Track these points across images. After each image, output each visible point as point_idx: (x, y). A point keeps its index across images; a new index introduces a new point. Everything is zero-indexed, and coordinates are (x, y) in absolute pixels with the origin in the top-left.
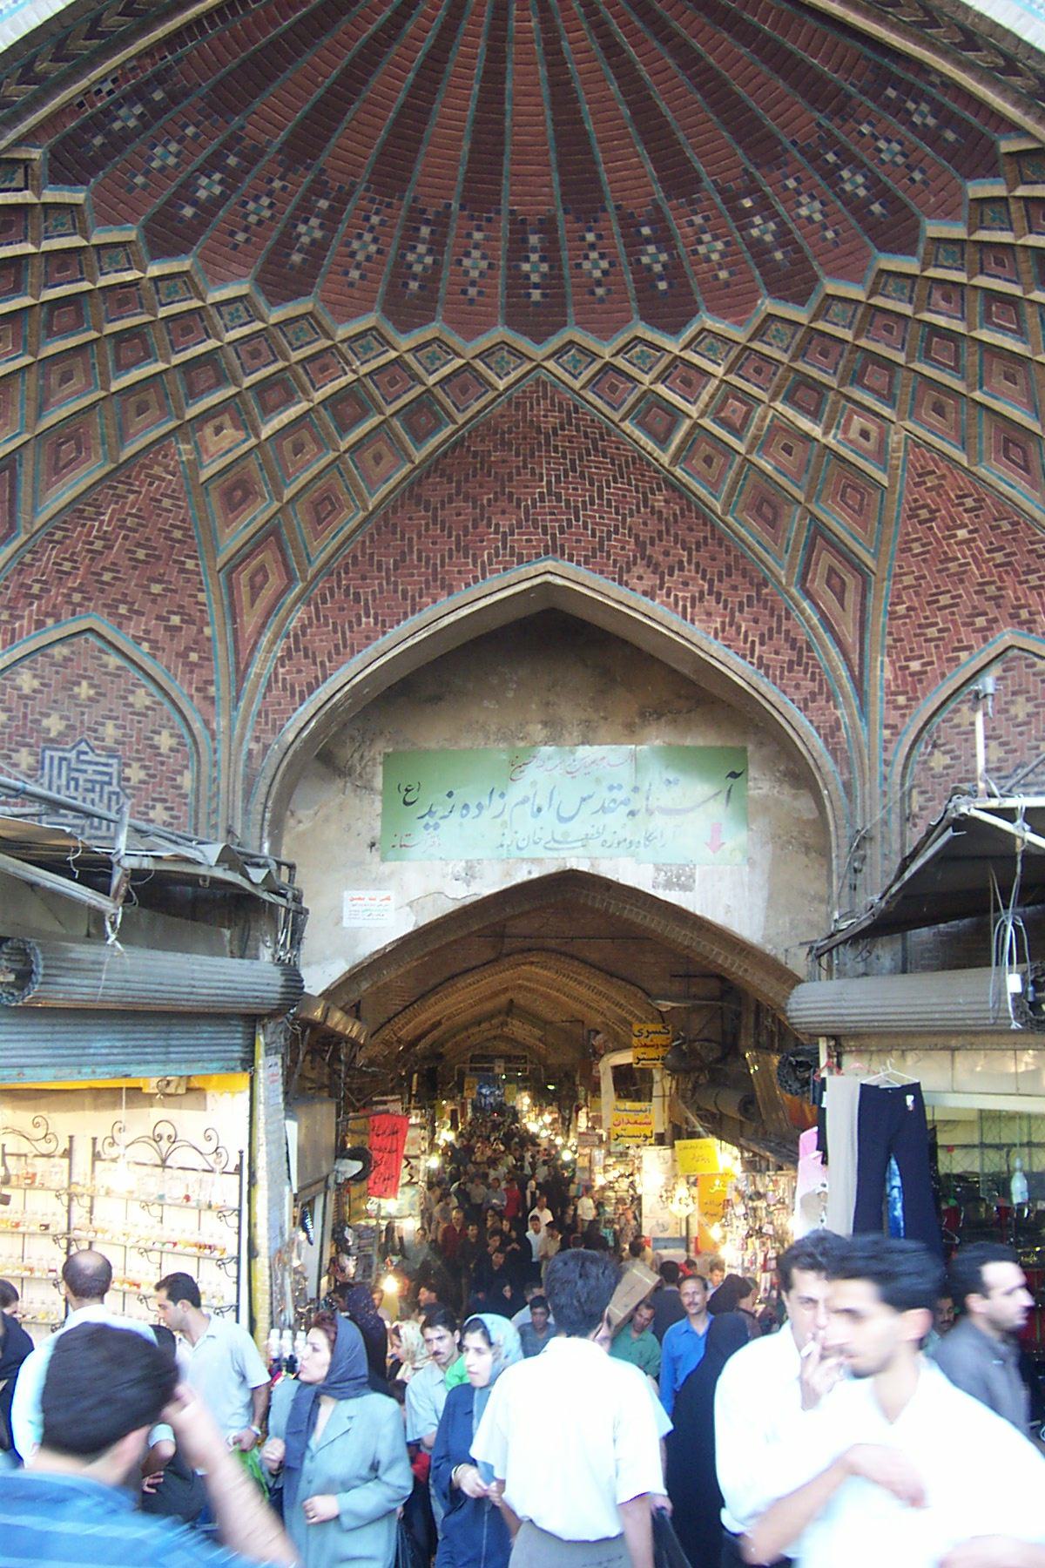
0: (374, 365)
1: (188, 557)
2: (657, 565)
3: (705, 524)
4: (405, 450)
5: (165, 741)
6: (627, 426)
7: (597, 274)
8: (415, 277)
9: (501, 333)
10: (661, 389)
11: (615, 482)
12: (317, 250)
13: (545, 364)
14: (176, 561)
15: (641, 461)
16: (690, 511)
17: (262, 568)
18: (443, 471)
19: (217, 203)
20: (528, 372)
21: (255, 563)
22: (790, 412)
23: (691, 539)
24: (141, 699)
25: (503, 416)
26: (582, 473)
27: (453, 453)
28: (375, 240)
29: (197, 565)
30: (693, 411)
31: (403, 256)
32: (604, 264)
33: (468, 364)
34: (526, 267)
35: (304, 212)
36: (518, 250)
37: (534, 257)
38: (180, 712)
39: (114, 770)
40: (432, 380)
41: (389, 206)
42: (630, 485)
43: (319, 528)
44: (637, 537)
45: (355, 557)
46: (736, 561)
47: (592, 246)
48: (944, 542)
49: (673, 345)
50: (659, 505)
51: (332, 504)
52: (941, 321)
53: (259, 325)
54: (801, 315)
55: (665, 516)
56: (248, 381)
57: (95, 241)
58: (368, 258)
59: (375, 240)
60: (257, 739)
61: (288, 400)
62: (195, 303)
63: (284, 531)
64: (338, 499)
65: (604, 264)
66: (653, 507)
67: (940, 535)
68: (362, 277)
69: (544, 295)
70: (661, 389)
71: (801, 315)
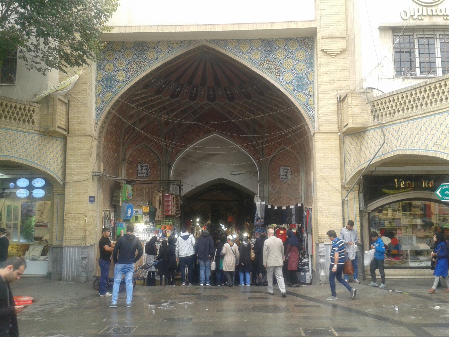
0: (188, 106)
5: (156, 161)
6: (226, 114)
8: (194, 94)
9: (206, 102)
10: (231, 109)
12: (179, 92)
15: (227, 119)
19: (165, 88)
22: (250, 114)
24: (152, 155)
30: (236, 113)
35: (177, 87)
38: (158, 156)
39: (148, 166)
47: (220, 91)
49: (232, 104)
52: (269, 105)
53: (171, 102)
54: (250, 101)
56: (169, 109)
57: (148, 95)
60: (170, 160)
61: (175, 111)
62: (162, 100)
70: (231, 109)
71: (250, 101)
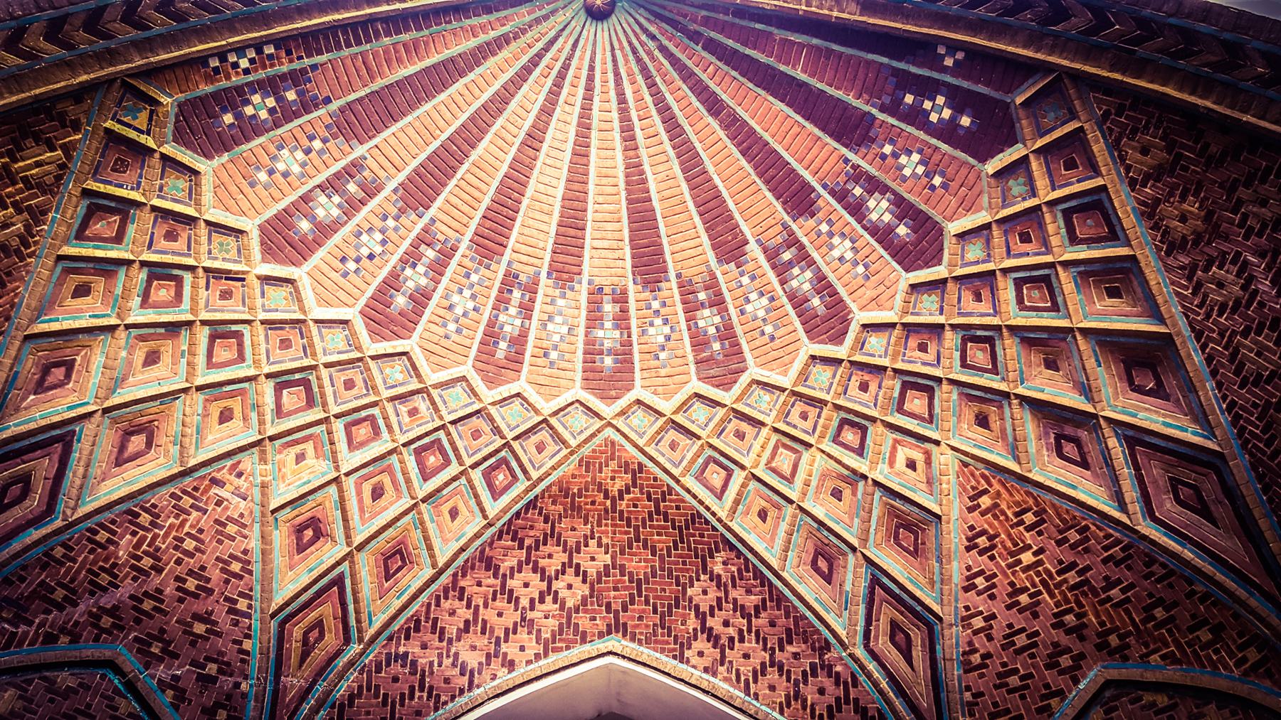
1: (242, 595)
2: (717, 638)
3: (762, 585)
4: (479, 504)
6: (689, 481)
7: (661, 339)
11: (676, 549)
13: (614, 422)
14: (227, 599)
16: (748, 571)
17: (319, 624)
18: (516, 533)
20: (599, 431)
21: (313, 616)
23: (752, 600)
25: (574, 476)
26: (645, 541)
27: (526, 513)
28: (473, 297)
29: (250, 607)
31: (497, 317)
32: (667, 330)
33: (545, 421)
34: (600, 333)
36: (594, 319)
37: (608, 325)
40: (510, 435)
41: (488, 268)
42: (690, 549)
43: (386, 585)
44: (697, 607)
45: (418, 622)
46: (796, 624)
48: (1009, 572)
50: (718, 569)
51: (403, 559)
55: (724, 580)
58: (465, 314)
59: (473, 297)
63: (348, 582)
64: (409, 554)
65: (667, 330)
66: (712, 572)
67: (1003, 564)
68: (458, 331)
69: (616, 361)
